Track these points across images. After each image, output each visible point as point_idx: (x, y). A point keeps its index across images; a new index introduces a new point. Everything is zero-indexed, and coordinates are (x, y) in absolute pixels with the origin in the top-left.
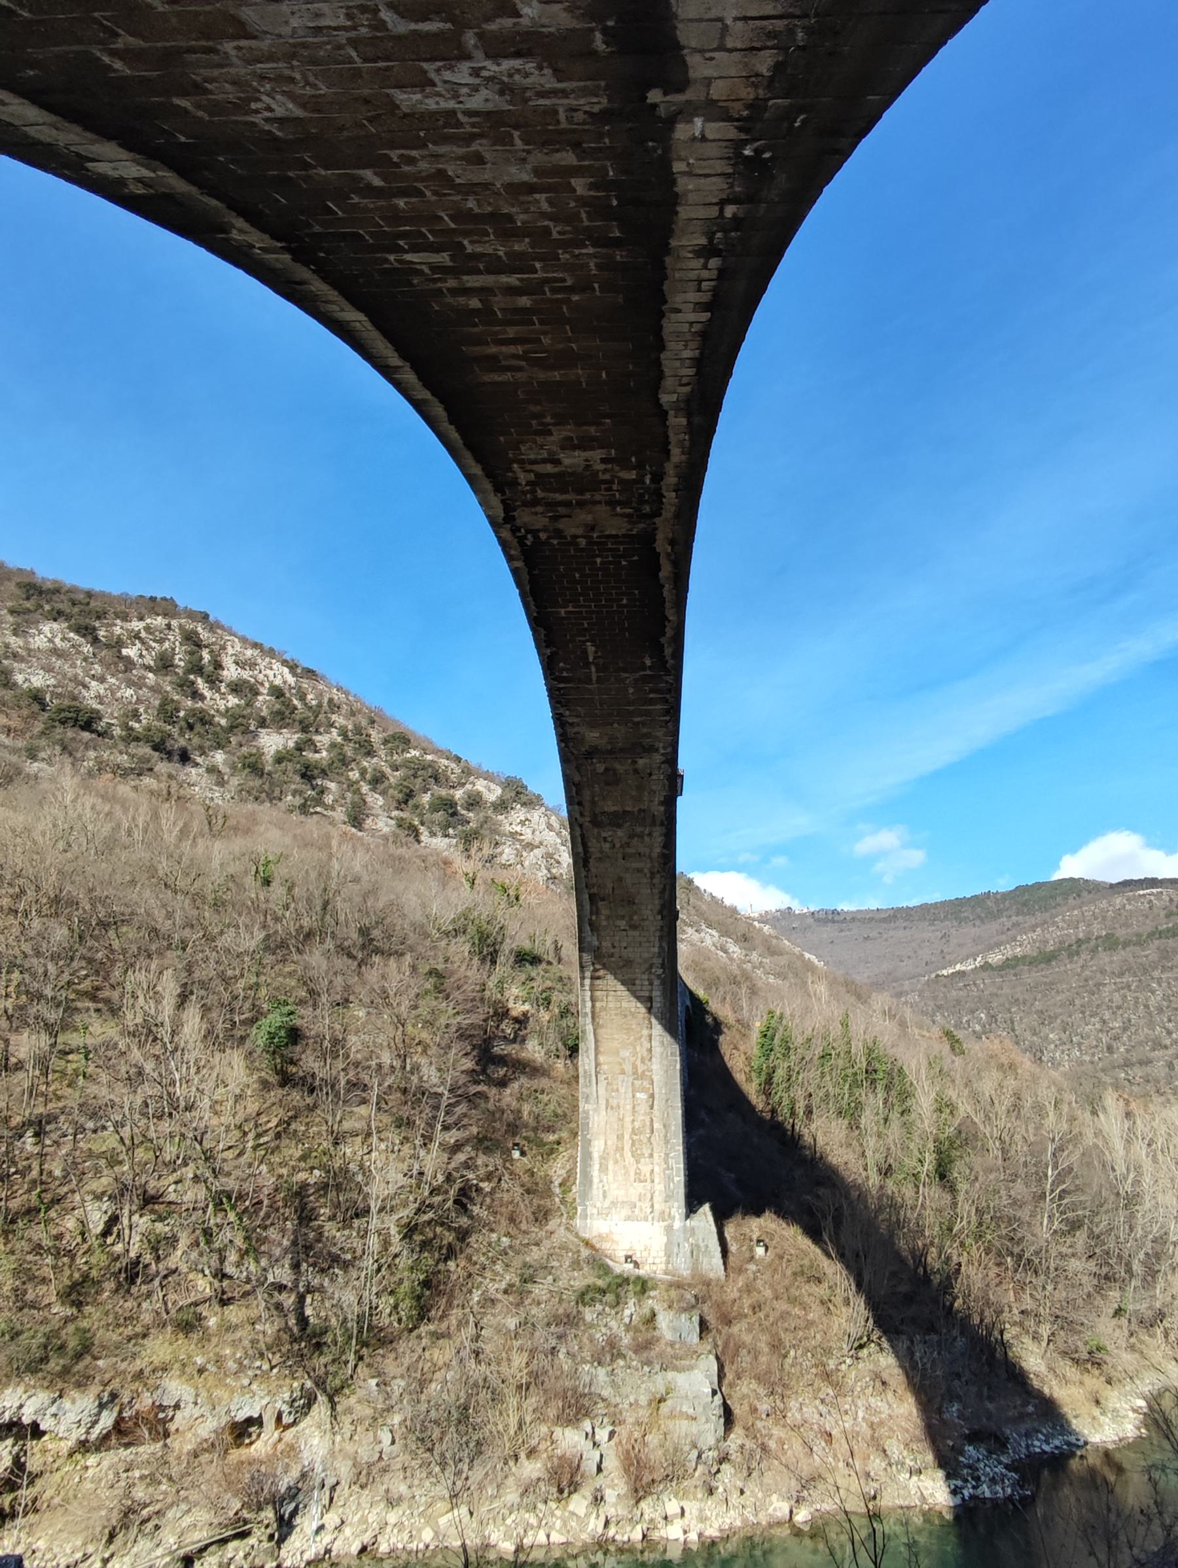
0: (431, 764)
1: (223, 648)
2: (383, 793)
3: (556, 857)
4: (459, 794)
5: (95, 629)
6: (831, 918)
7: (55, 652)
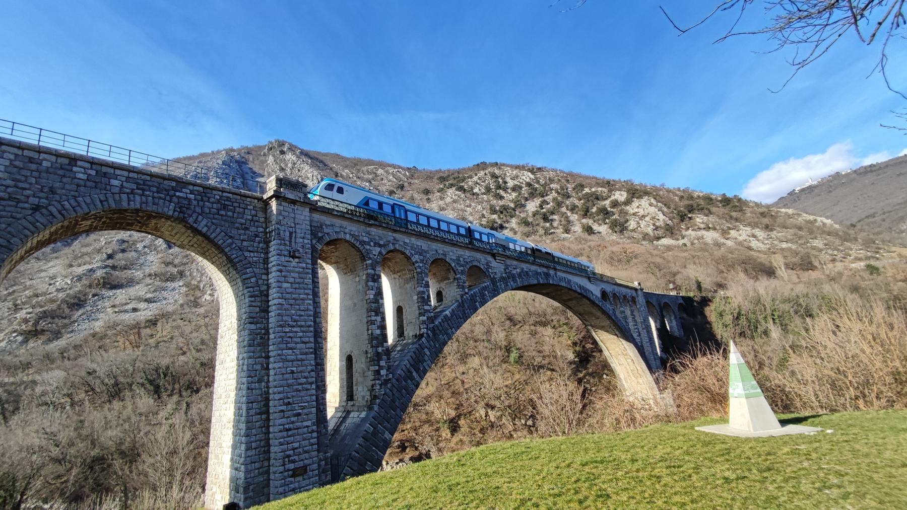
1: (505, 174)
2: (576, 213)
3: (657, 217)
4: (607, 203)
5: (463, 186)
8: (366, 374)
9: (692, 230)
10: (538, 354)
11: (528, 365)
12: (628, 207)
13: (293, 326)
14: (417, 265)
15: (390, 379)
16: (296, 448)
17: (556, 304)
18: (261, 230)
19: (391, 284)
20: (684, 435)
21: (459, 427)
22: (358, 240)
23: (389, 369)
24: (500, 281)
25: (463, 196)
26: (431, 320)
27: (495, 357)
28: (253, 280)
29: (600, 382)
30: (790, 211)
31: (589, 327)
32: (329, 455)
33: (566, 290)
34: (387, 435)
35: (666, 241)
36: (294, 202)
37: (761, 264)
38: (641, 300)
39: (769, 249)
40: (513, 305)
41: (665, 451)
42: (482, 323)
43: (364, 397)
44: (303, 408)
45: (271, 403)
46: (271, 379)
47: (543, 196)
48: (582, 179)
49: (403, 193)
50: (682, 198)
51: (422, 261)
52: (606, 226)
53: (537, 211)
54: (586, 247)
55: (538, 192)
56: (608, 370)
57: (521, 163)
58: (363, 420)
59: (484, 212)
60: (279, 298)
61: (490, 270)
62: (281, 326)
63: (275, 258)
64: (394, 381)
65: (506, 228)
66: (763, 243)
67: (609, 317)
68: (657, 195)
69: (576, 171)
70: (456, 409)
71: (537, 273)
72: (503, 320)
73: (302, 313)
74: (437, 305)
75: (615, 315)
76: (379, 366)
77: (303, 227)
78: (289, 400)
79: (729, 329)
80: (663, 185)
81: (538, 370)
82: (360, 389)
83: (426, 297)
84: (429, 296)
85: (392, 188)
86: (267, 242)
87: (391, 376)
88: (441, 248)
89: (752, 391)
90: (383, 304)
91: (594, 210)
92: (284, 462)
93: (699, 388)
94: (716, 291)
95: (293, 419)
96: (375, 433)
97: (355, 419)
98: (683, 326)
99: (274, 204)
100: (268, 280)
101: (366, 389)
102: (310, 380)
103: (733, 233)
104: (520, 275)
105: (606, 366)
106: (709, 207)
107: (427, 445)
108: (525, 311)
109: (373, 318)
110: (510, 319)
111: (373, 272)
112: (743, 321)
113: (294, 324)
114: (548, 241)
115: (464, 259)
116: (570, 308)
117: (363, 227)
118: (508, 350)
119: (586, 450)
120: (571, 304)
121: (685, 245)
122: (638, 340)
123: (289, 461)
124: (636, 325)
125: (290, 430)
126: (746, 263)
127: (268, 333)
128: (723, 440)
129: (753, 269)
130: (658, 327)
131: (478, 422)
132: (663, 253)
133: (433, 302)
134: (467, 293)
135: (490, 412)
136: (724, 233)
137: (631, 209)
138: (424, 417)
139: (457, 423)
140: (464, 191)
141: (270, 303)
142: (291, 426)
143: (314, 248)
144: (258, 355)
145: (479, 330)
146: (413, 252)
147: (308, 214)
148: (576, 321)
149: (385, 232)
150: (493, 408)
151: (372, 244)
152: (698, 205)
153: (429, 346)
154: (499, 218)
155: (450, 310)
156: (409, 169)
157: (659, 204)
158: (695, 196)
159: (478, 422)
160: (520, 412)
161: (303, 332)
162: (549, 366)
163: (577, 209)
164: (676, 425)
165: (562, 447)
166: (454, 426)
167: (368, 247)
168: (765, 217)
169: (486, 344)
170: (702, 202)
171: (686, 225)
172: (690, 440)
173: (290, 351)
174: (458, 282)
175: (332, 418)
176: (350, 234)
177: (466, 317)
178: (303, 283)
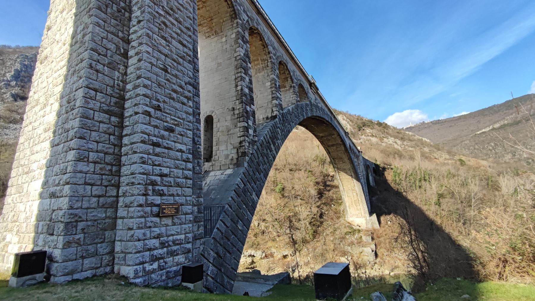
6: (438, 122)
80: (347, 112)
171: (361, 133)
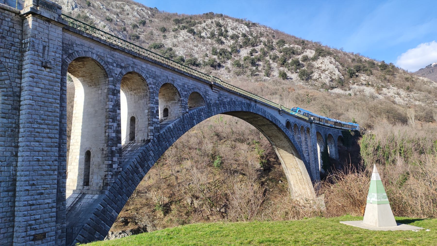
0: (291, 49)
1: (227, 25)
2: (277, 62)
3: (334, 72)
4: (300, 57)
5: (193, 30)
7: (185, 41)
8: (100, 167)
9: (357, 85)
10: (235, 162)
11: (227, 169)
12: (314, 63)
13: (41, 124)
14: (150, 86)
15: (120, 172)
16: (38, 219)
17: (253, 127)
18: (17, 40)
19: (127, 99)
20: (332, 226)
21: (171, 210)
22: (103, 60)
23: (120, 164)
24: (213, 106)
25: (192, 37)
26: (157, 130)
27: (203, 162)
28: (7, 82)
29: (276, 185)
30: (426, 79)
31: (274, 146)
32: (65, 225)
33: (261, 118)
34: (114, 213)
35: (337, 91)
36: (48, 20)
37: (399, 114)
38: (313, 130)
39: (407, 104)
40: (221, 125)
41: (318, 236)
42: (196, 136)
43: (97, 184)
44: (46, 189)
45: (18, 184)
46: (19, 164)
47: (253, 46)
48: (284, 36)
49: (144, 28)
50: (354, 60)
51: (154, 84)
52: (297, 74)
53: (248, 57)
54: (280, 88)
55: (250, 42)
56: (284, 178)
57: (240, 18)
58: (95, 201)
59: (208, 52)
60: (30, 100)
61: (207, 97)
62: (30, 122)
63: (29, 66)
64: (123, 173)
65: (223, 67)
66: (403, 100)
67: (289, 140)
68: (336, 56)
69: (281, 30)
70: (169, 197)
71: (242, 103)
72: (212, 135)
73: (50, 114)
74: (163, 119)
75: (294, 139)
76: (112, 161)
77: (56, 43)
78: (34, 182)
79: (369, 157)
80: (342, 49)
81: (234, 174)
82: (95, 177)
83: (155, 112)
84: (157, 111)
85: (135, 23)
86: (22, 52)
87: (121, 169)
88: (171, 75)
89: (382, 200)
90: (120, 114)
91: (290, 61)
92: (26, 229)
93: (346, 195)
94: (365, 130)
95: (36, 197)
96: (104, 212)
97: (89, 200)
98: (340, 152)
99: (30, 19)
100: (21, 83)
101: (100, 178)
102: (53, 167)
103: (385, 90)
104: (229, 103)
105: (282, 176)
106: (371, 69)
107: (145, 221)
108: (229, 130)
109: (111, 124)
110: (218, 135)
111: (113, 87)
112: (380, 153)
113: (42, 122)
114: (253, 81)
115: (188, 86)
116: (262, 131)
117: (108, 50)
118: (213, 157)
119: (263, 232)
120: (264, 128)
121: (350, 95)
122: (307, 158)
123: (31, 228)
124: (307, 148)
125: (33, 205)
126: (389, 113)
127: (18, 127)
128: (358, 231)
129: (394, 117)
130: (322, 151)
131: (185, 207)
132: (334, 99)
133: (160, 116)
134: (187, 112)
135: (195, 201)
136: (379, 89)
137: (316, 64)
138: (144, 201)
139: (169, 207)
140: (194, 33)
141: (22, 103)
142: (34, 202)
143: (64, 63)
144: (9, 144)
145: (193, 141)
146: (148, 76)
147: (61, 33)
148: (265, 141)
149: (126, 57)
150: (197, 198)
151: (115, 65)
152: (364, 67)
153: (154, 150)
154: (219, 58)
155: (173, 123)
156: (151, 9)
157: (337, 63)
158: (363, 60)
159: (185, 207)
160: (217, 202)
161: (49, 129)
162: (242, 172)
163: (277, 59)
164: (326, 219)
165: (246, 229)
166: (167, 209)
167: (111, 67)
168: (408, 81)
169: (198, 152)
170: (367, 65)
171: (353, 80)
172: (336, 230)
173: (38, 143)
174: (181, 103)
175: (70, 197)
176: (97, 55)
177: (184, 130)
178: (52, 89)
